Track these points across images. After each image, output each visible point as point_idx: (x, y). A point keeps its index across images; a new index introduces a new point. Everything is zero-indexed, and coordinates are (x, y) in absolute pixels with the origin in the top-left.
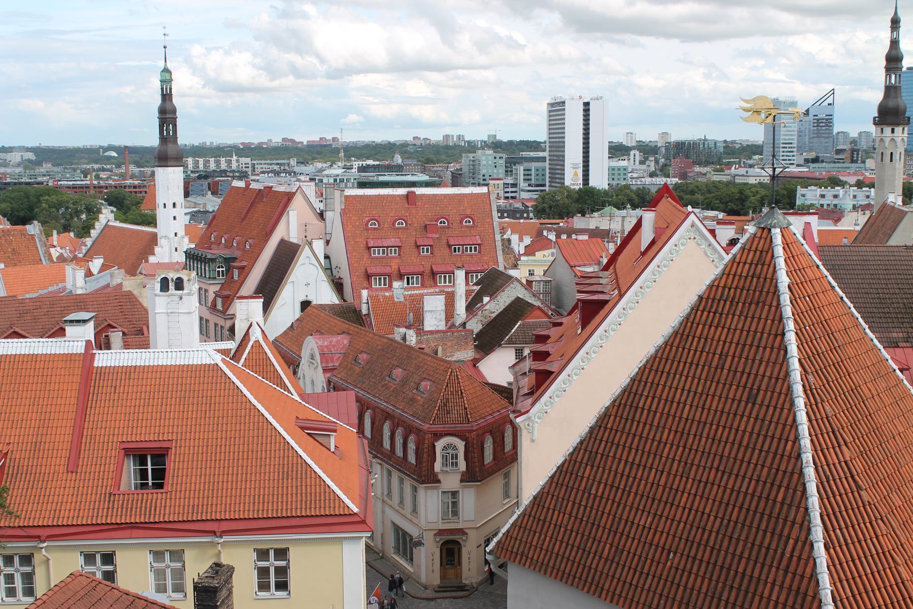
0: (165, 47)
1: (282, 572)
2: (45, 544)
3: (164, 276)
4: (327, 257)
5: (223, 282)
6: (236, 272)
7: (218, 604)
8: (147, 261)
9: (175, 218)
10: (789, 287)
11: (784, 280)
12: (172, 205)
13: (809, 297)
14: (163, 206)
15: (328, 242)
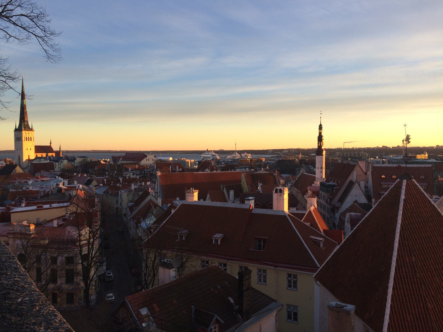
0: (321, 118)
1: (295, 283)
2: (229, 261)
3: (276, 188)
4: (366, 187)
5: (330, 193)
6: (334, 190)
7: (244, 280)
8: (312, 186)
9: (321, 172)
10: (404, 200)
11: (403, 197)
12: (321, 168)
13: (414, 204)
14: (317, 168)
15: (367, 182)
